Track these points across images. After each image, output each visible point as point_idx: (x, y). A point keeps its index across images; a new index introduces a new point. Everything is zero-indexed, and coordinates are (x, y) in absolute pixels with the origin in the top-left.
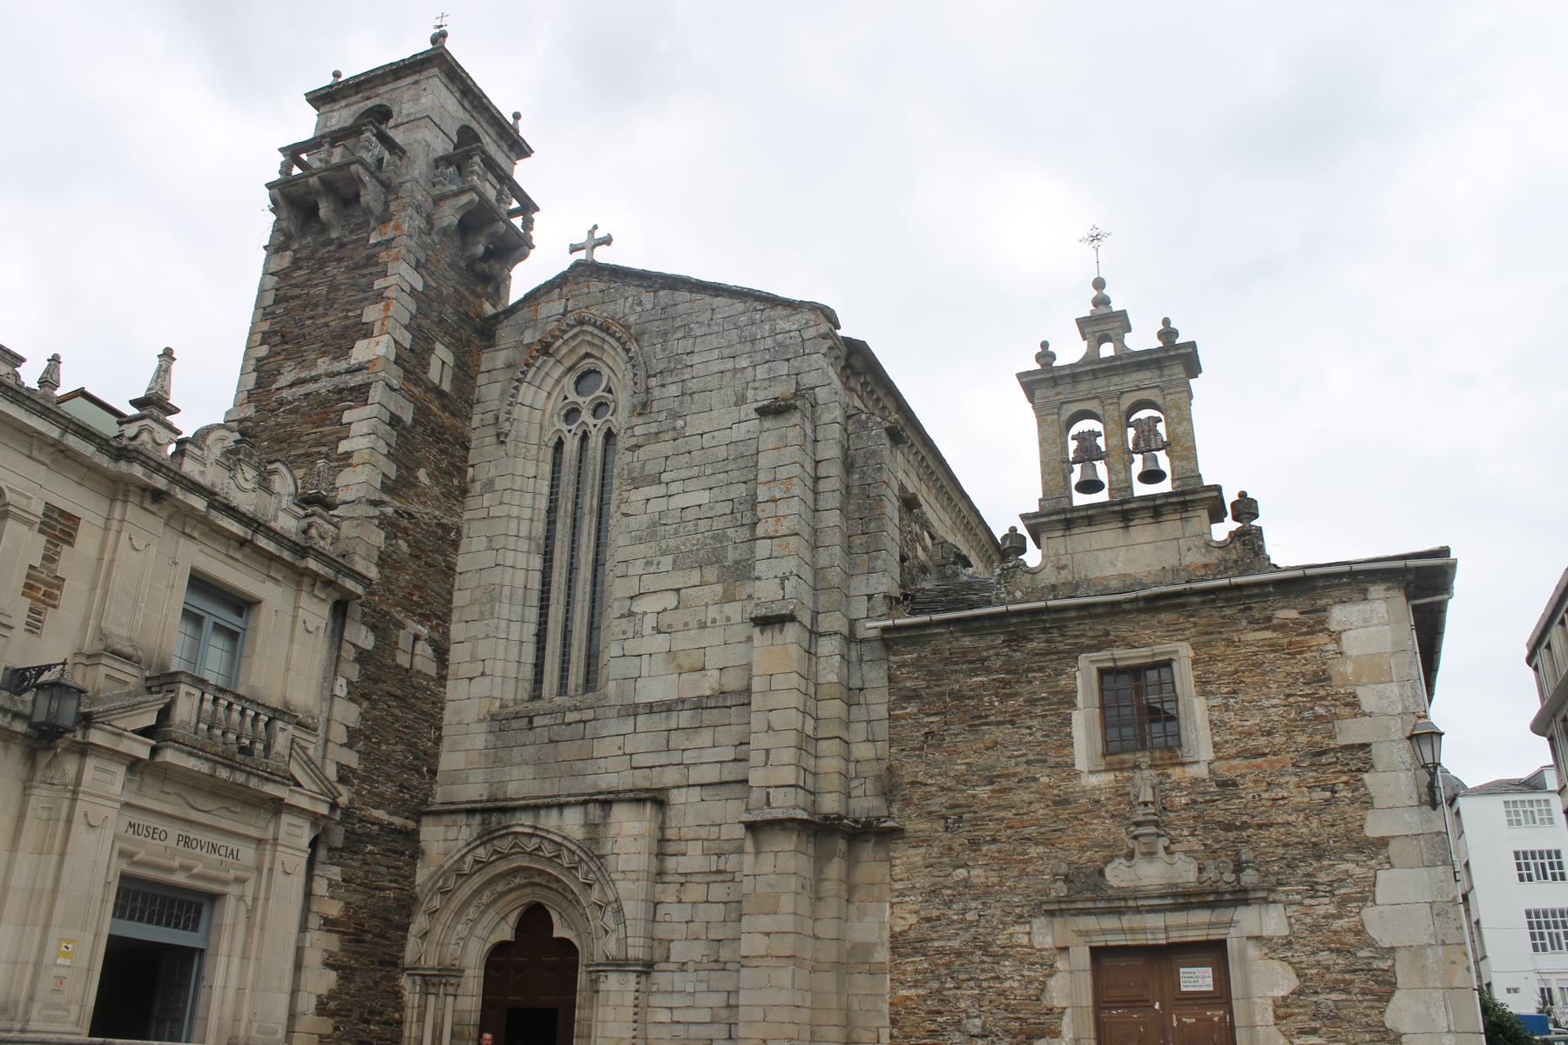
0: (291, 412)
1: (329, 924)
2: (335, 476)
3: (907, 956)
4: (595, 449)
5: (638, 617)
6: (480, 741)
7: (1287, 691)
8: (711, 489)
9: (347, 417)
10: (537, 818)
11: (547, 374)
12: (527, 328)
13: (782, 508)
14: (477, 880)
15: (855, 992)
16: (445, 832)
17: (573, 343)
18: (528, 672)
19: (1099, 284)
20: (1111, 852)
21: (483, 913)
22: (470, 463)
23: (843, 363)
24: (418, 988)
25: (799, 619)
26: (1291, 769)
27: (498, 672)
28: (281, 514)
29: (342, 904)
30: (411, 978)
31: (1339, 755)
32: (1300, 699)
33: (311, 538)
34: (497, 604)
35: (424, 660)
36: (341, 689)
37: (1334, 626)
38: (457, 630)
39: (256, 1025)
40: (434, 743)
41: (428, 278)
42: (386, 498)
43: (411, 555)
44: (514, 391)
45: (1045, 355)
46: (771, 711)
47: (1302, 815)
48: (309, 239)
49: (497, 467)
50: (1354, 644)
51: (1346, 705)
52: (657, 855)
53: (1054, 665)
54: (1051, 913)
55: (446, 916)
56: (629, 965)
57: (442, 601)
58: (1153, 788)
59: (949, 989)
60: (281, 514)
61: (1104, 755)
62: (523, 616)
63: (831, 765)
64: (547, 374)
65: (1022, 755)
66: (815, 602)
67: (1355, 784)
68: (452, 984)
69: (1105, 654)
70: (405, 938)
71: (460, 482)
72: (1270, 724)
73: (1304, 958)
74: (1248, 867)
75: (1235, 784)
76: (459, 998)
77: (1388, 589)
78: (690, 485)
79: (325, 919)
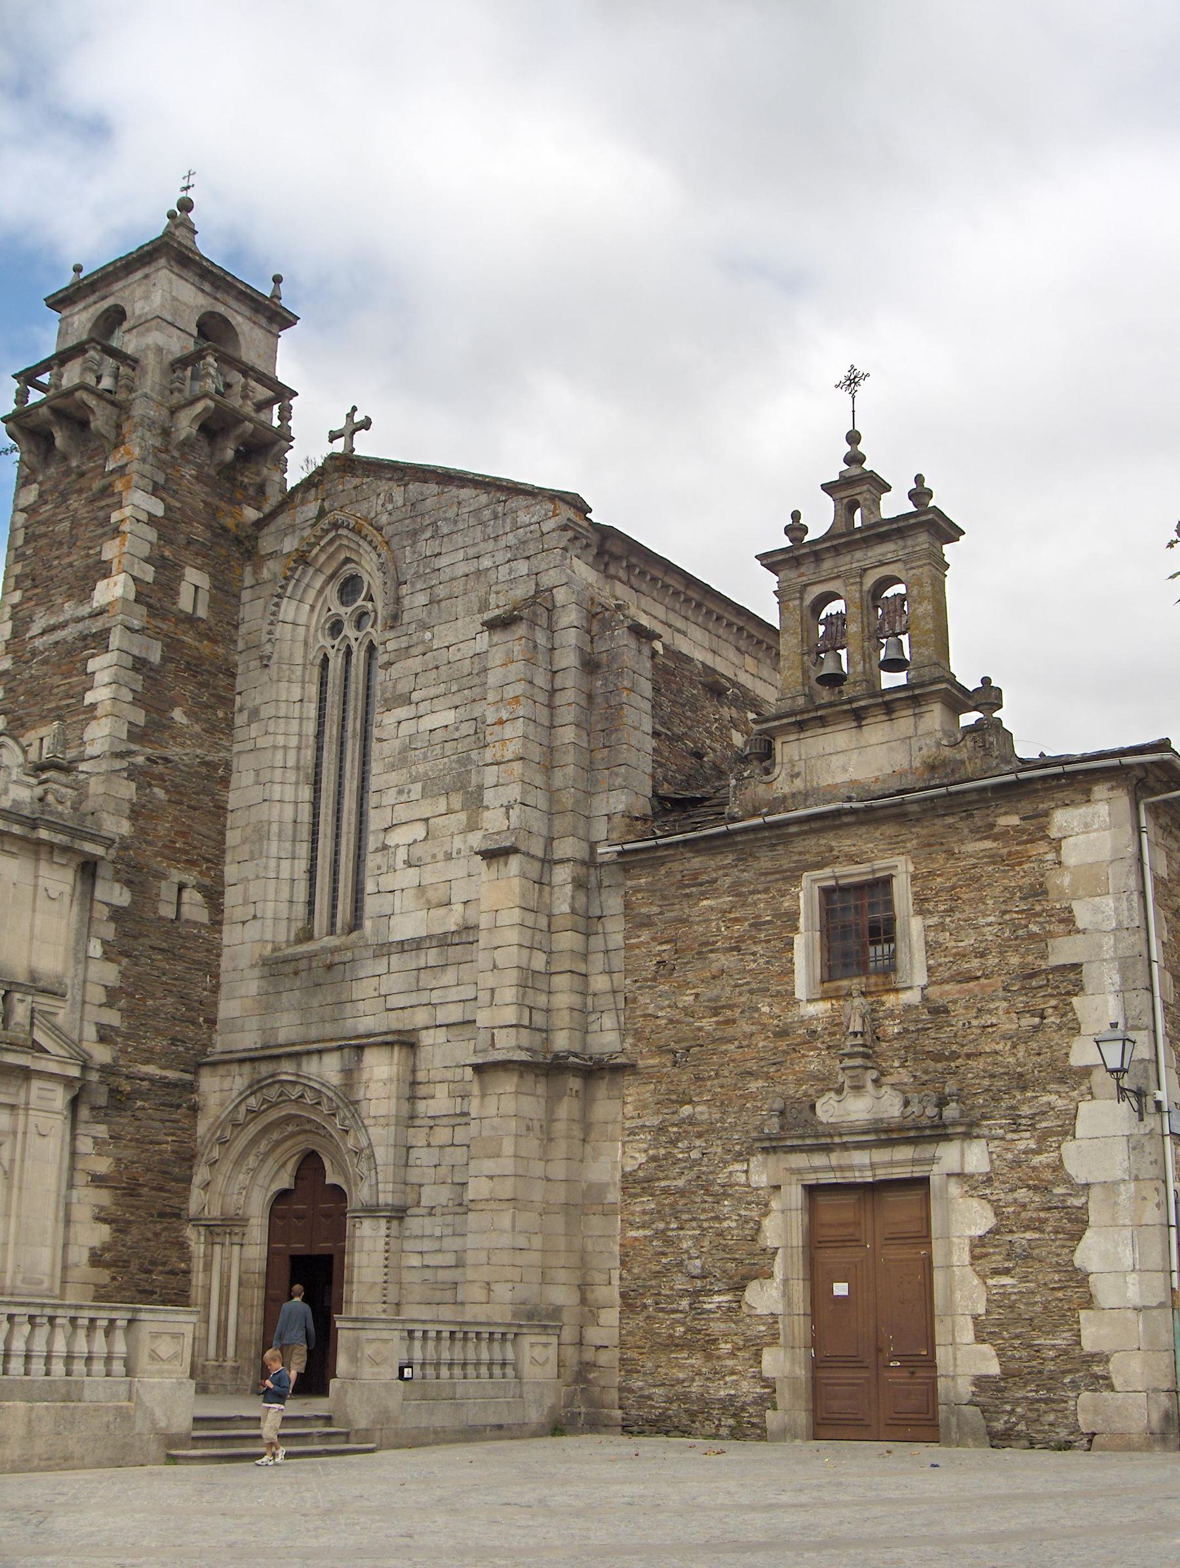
0: (45, 662)
1: (98, 1180)
2: (83, 730)
3: (635, 1195)
4: (357, 667)
5: (391, 850)
6: (253, 987)
7: (1003, 907)
8: (456, 707)
9: (92, 665)
10: (299, 1065)
11: (308, 585)
12: (286, 535)
13: (509, 731)
14: (252, 1130)
15: (591, 1233)
17: (331, 549)
18: (300, 910)
19: (853, 438)
20: (827, 1084)
21: (263, 1161)
22: (238, 690)
23: (595, 551)
24: (202, 1239)
25: (523, 849)
26: (1001, 993)
27: (269, 914)
28: (12, 787)
29: (111, 1160)
31: (1051, 976)
32: (1015, 916)
33: (48, 805)
34: (265, 842)
35: (194, 908)
36: (95, 949)
37: (1054, 833)
38: (231, 872)
39: (20, 1277)
40: (211, 991)
41: (170, 500)
42: (134, 747)
43: (169, 801)
44: (274, 608)
45: (796, 529)
46: (496, 948)
47: (1009, 1044)
48: (53, 469)
49: (262, 693)
50: (1072, 854)
51: (1061, 921)
52: (408, 1099)
53: (780, 885)
54: (765, 1150)
55: (226, 1167)
56: (380, 1211)
57: (212, 843)
58: (863, 1017)
59: (673, 1230)
60: (12, 787)
61: (823, 982)
62: (293, 852)
63: (564, 1000)
64: (308, 585)
65: (748, 983)
66: (550, 827)
67: (1065, 1009)
68: (236, 1234)
69: (827, 871)
70: (188, 1190)
71: (226, 713)
72: (983, 945)
73: (1002, 1196)
74: (953, 1101)
75: (947, 1011)
76: (245, 1248)
77: (1112, 789)
78: (439, 704)
79: (93, 1176)
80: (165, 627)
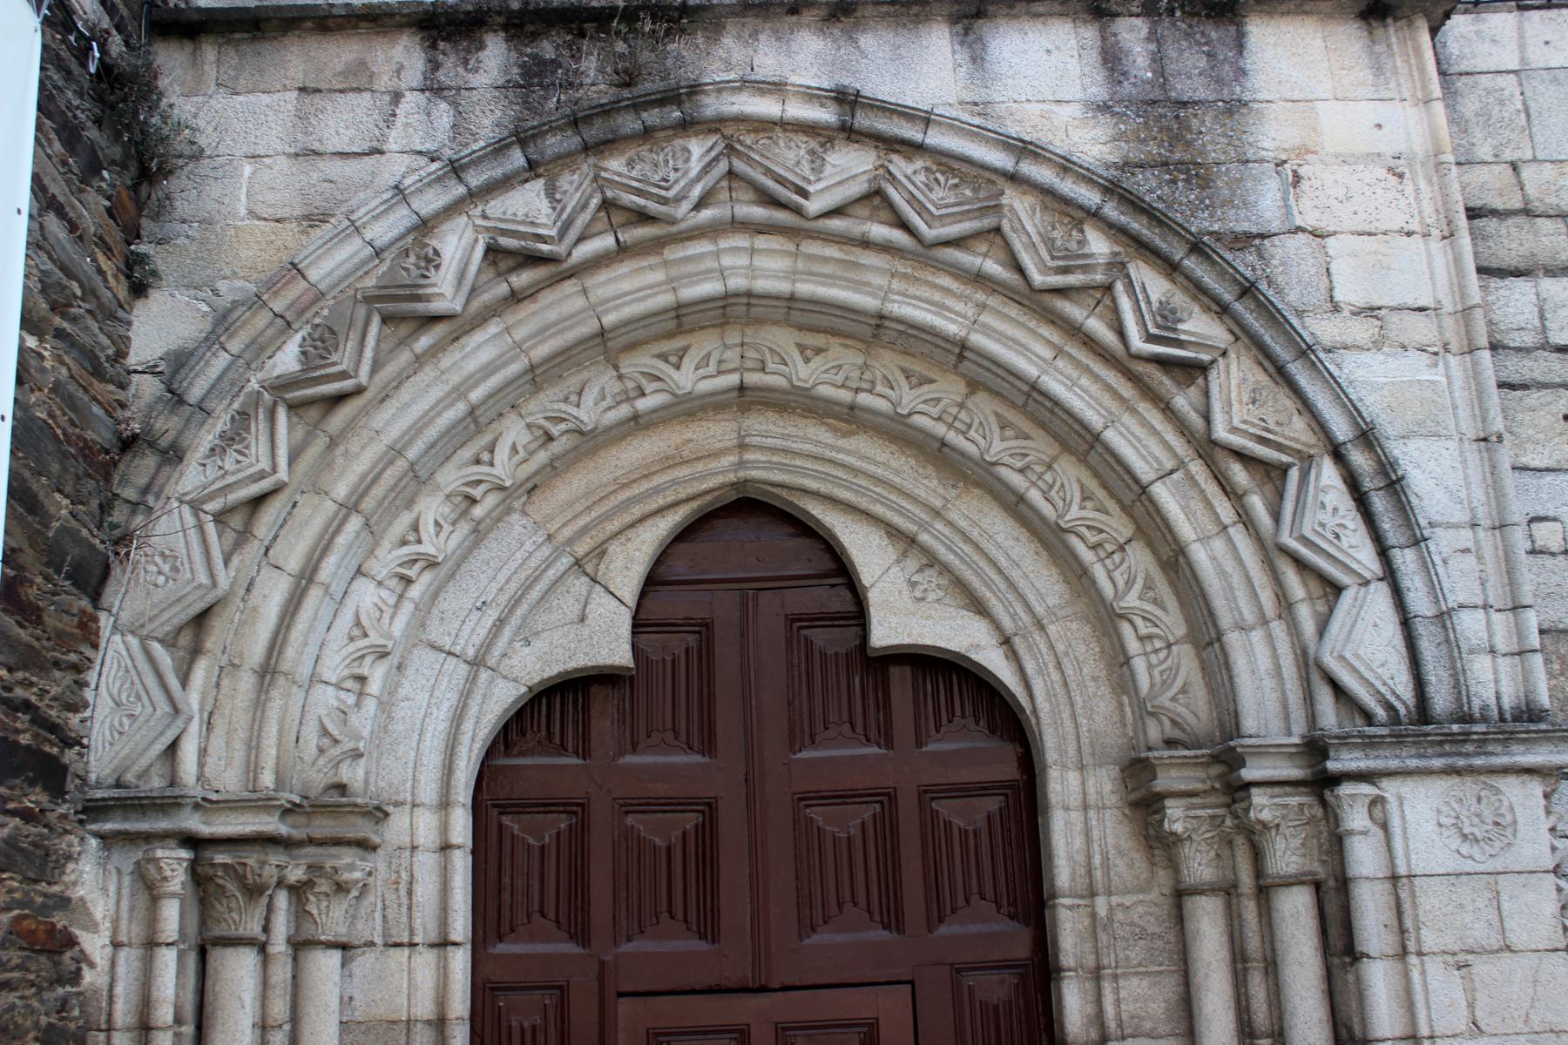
16: (301, 116)
21: (479, 534)
24: (171, 916)
30: (126, 859)
70: (88, 632)
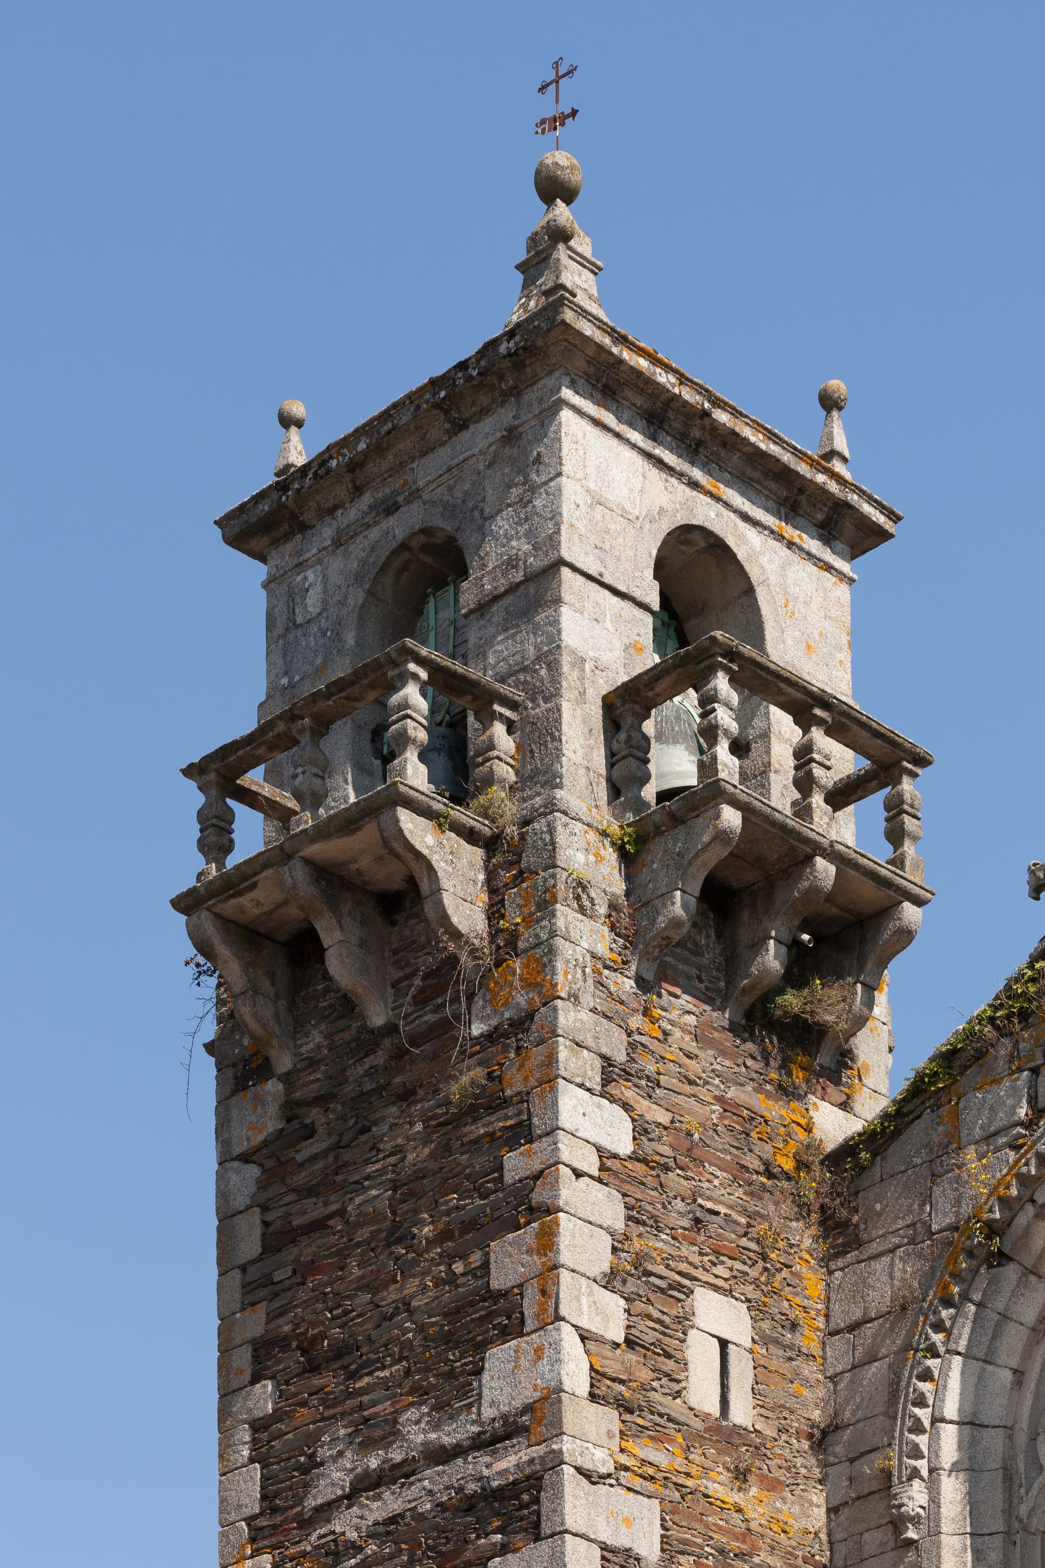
41: (643, 1105)
80: (661, 1458)
